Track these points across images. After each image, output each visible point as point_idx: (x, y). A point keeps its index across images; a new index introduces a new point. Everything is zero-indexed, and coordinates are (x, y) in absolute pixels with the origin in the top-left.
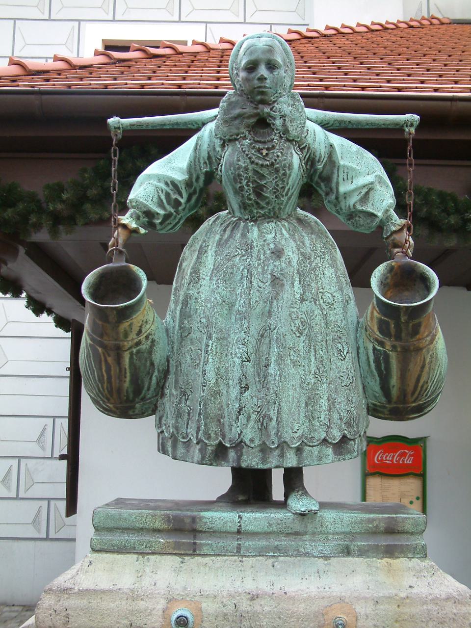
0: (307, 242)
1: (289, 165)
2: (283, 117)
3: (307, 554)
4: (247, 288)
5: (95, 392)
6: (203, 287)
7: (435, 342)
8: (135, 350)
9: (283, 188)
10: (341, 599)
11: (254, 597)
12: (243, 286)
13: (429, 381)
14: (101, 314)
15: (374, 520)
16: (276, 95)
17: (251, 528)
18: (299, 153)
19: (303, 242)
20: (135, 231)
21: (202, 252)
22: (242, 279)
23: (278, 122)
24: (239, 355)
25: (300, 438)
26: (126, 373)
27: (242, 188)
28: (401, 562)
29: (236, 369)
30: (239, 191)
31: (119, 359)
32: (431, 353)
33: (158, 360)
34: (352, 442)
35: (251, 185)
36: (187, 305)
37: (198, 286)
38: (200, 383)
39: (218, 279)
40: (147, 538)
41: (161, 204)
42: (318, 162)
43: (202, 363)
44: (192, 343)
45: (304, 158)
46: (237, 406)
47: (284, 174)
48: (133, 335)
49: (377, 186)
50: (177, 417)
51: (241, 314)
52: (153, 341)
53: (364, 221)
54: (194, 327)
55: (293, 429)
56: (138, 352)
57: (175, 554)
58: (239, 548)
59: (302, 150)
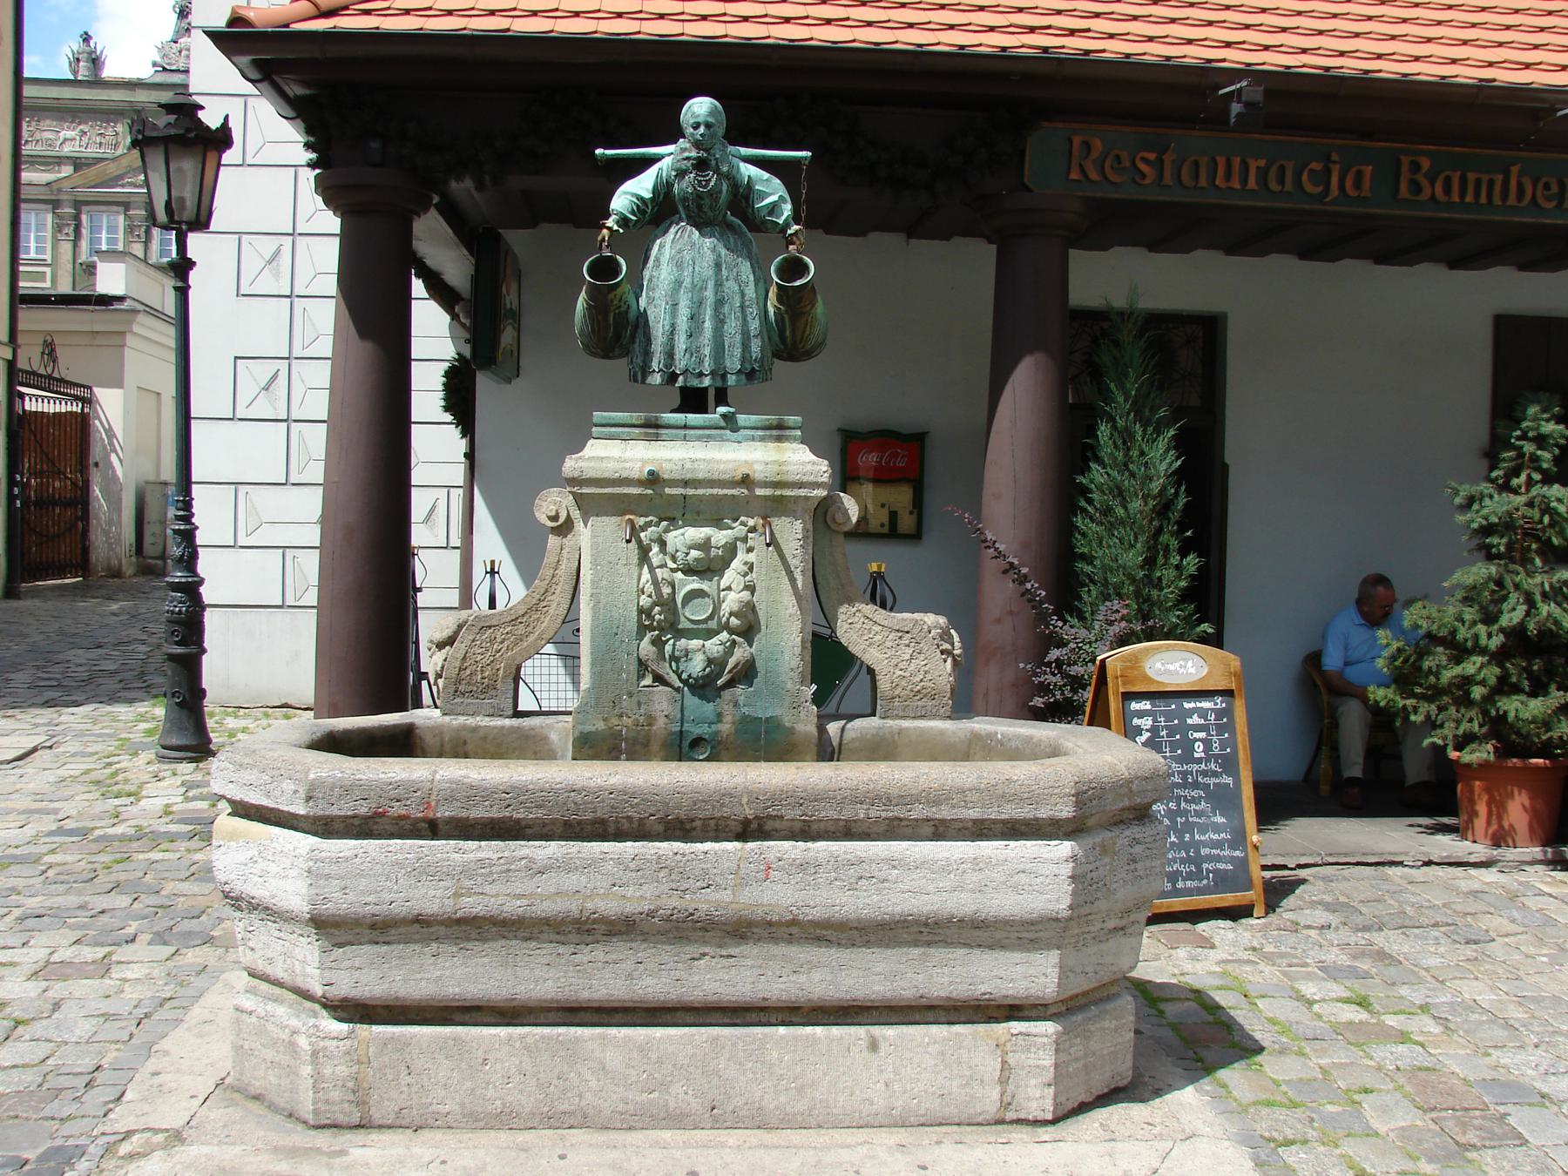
0: (732, 240)
2: (716, 159)
3: (728, 440)
10: (746, 462)
17: (693, 424)
21: (661, 246)
23: (713, 163)
30: (686, 208)
31: (606, 317)
41: (633, 213)
48: (616, 302)
54: (657, 296)
59: (729, 180)
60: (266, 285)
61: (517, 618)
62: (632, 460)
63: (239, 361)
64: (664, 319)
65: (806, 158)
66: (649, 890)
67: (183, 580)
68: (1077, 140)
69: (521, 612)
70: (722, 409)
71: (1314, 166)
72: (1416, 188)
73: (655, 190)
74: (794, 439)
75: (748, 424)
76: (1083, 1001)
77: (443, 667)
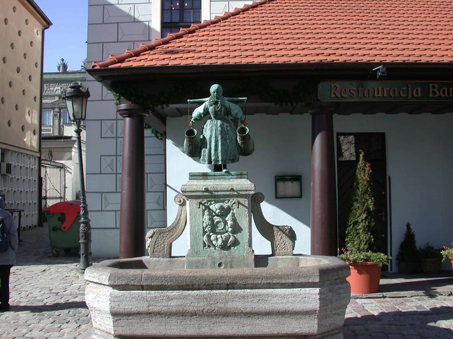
14: (189, 138)
17: (216, 175)
25: (225, 159)
40: (198, 177)
48: (195, 142)
52: (198, 143)
58: (215, 178)
60: (109, 134)
61: (170, 230)
63: (102, 157)
65: (245, 100)
66: (201, 304)
67: (84, 221)
68: (332, 85)
69: (171, 229)
70: (224, 170)
71: (403, 88)
72: (434, 93)
76: (326, 334)
77: (150, 244)
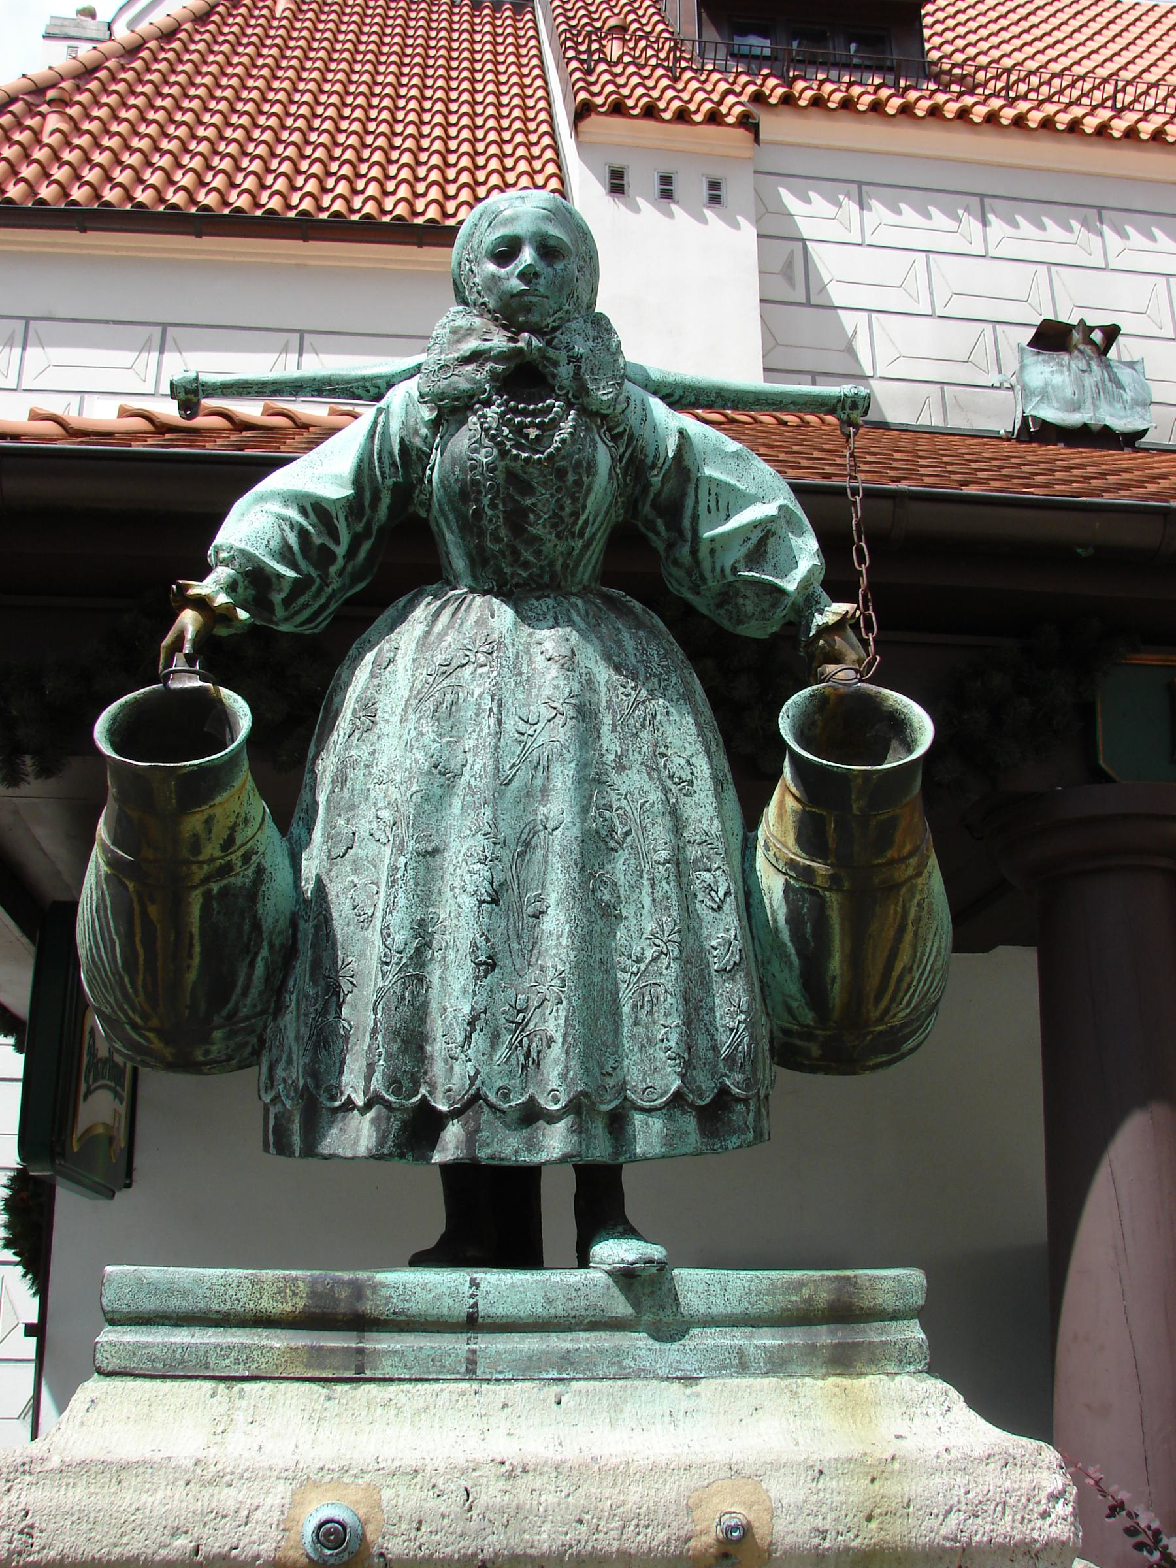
0: (629, 643)
1: (589, 463)
2: (575, 359)
3: (642, 1374)
4: (489, 734)
5: (112, 1001)
6: (385, 740)
7: (925, 874)
8: (215, 887)
9: (575, 515)
10: (734, 1471)
11: (513, 1473)
12: (482, 730)
13: (915, 967)
15: (801, 1284)
16: (559, 314)
17: (502, 1309)
18: (611, 444)
19: (619, 643)
20: (228, 611)
22: (477, 715)
23: (565, 371)
24: (471, 888)
26: (191, 945)
27: (478, 513)
28: (870, 1384)
29: (463, 922)
30: (470, 527)
32: (918, 897)
33: (270, 920)
34: (741, 1107)
35: (501, 506)
36: (343, 783)
37: (372, 737)
38: (375, 957)
39: (420, 718)
42: (653, 466)
43: (379, 914)
44: (356, 870)
45: (622, 457)
46: (467, 1009)
47: (578, 483)
48: (211, 850)
49: (782, 528)
50: (316, 1046)
51: (475, 793)
53: (756, 605)
54: (363, 832)
55: (602, 1067)
56: (225, 892)
57: (311, 1380)
58: (472, 1362)
59: (615, 438)
62: (249, 1476)
64: (390, 908)
73: (362, 476)
74: (902, 1358)
75: (719, 1306)
